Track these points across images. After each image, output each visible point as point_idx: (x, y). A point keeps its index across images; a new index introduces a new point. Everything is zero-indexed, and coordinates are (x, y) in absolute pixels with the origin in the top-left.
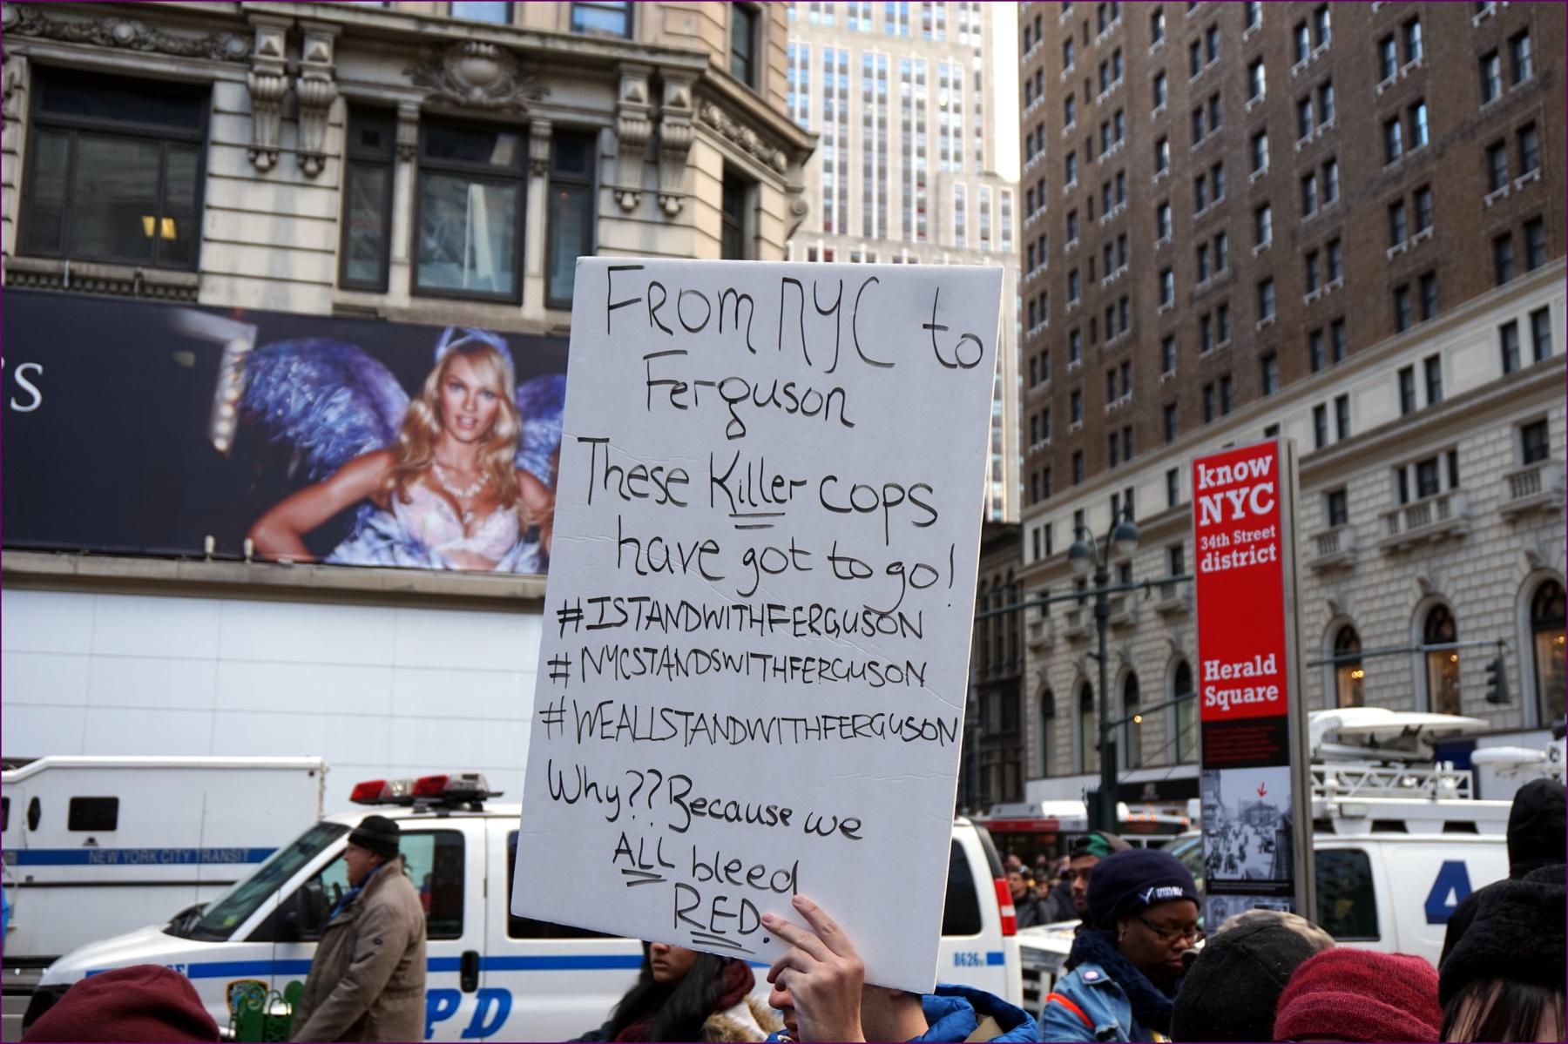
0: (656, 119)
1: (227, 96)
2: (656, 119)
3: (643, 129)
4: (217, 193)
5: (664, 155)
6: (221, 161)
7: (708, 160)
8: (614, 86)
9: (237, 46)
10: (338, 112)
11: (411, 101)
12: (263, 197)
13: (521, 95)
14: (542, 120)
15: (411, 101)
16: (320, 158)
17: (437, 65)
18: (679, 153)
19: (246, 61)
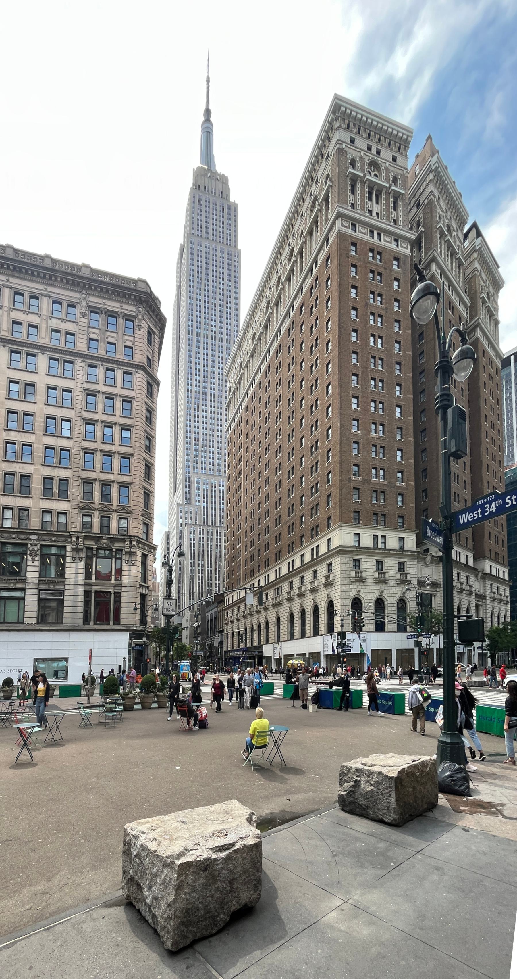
0: (130, 548)
1: (68, 548)
2: (130, 548)
3: (128, 550)
4: (67, 565)
5: (131, 554)
6: (68, 559)
7: (139, 553)
8: (125, 542)
9: (69, 540)
10: (85, 550)
11: (95, 547)
12: (74, 565)
13: (111, 545)
14: (114, 549)
15: (95, 547)
16: (82, 558)
17: (98, 541)
18: (134, 554)
19: (71, 542)
